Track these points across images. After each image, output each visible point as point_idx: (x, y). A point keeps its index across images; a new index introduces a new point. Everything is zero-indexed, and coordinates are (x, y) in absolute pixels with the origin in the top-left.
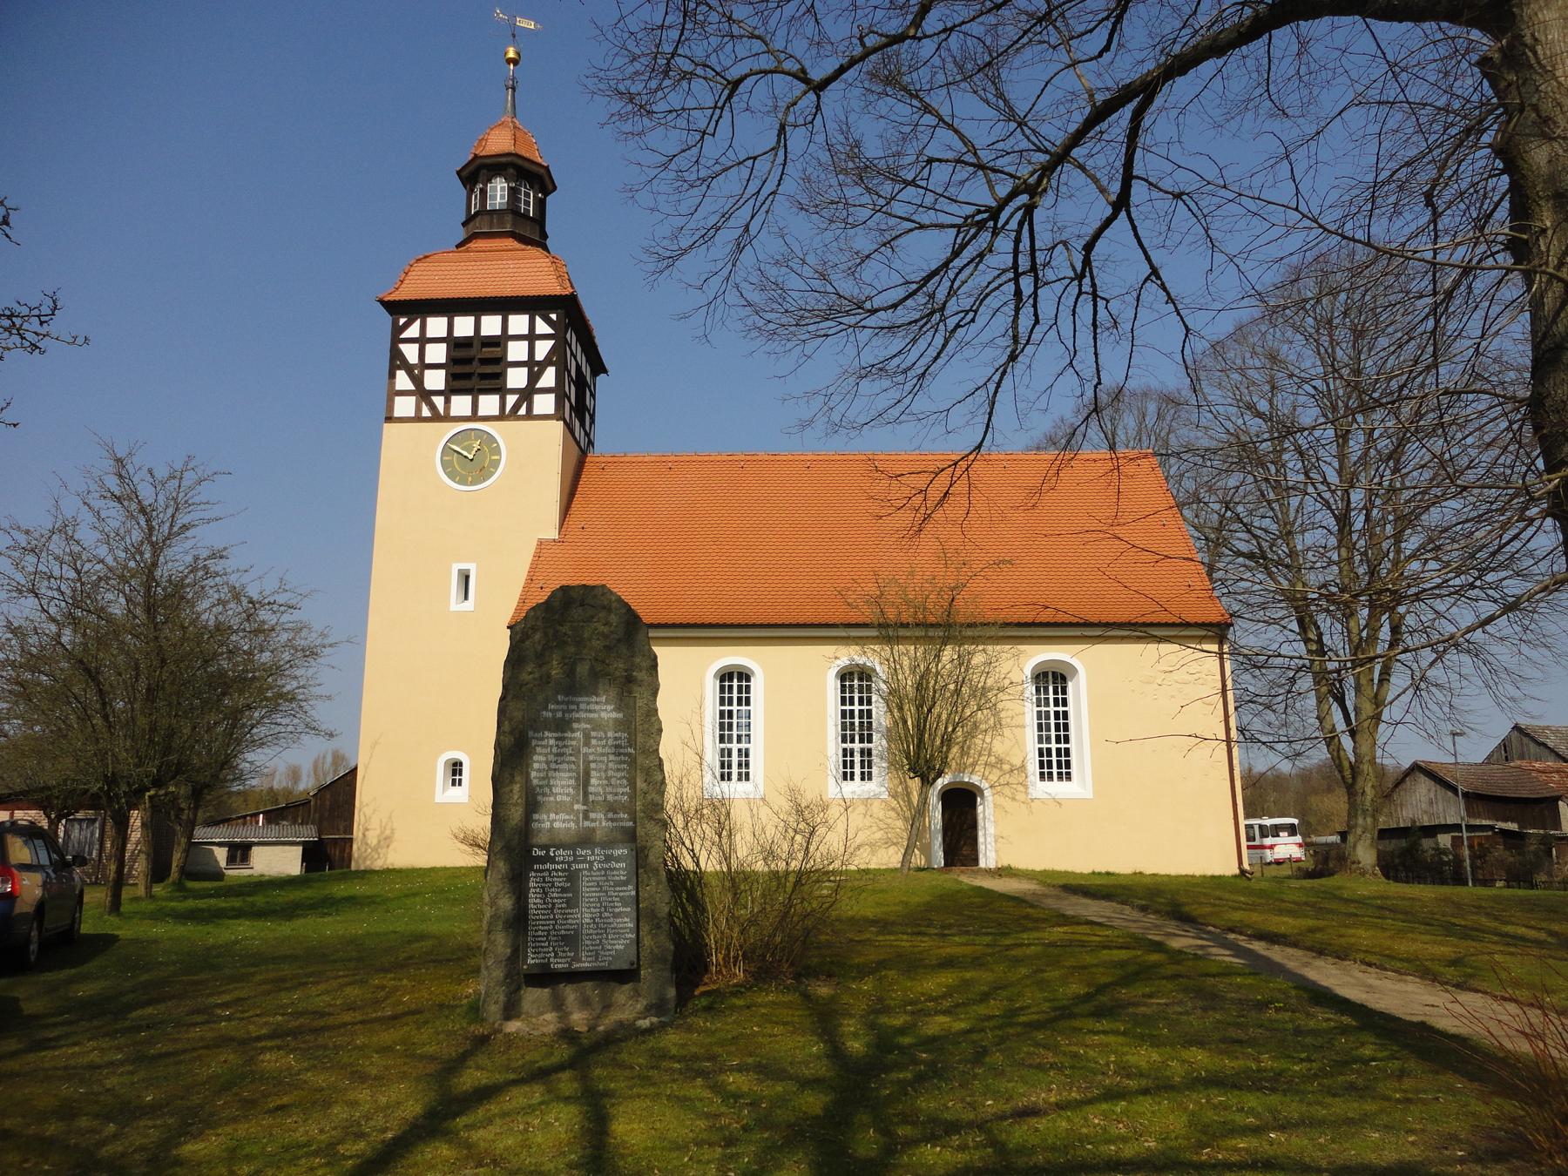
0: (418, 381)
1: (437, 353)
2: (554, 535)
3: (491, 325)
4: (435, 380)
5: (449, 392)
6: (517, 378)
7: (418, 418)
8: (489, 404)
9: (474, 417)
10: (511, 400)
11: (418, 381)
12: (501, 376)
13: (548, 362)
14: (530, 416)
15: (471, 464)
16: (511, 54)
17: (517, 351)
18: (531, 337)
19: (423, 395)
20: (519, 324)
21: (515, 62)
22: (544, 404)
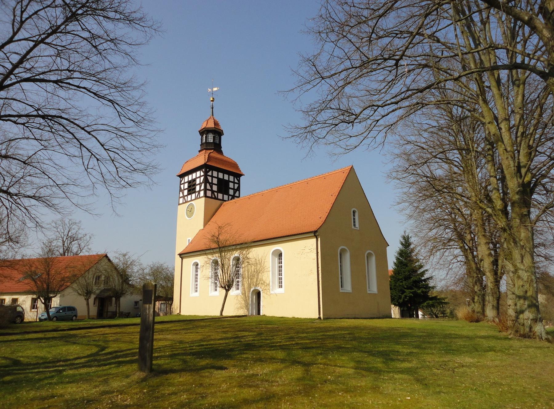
0: (183, 193)
1: (186, 186)
2: (202, 228)
3: (226, 177)
4: (186, 192)
5: (188, 194)
6: (198, 188)
7: (183, 203)
8: (193, 195)
9: (191, 200)
10: (197, 194)
11: (183, 193)
12: (195, 188)
13: (203, 182)
14: (200, 198)
15: (190, 212)
16: (211, 99)
17: (198, 181)
18: (200, 177)
19: (184, 197)
20: (198, 173)
21: (213, 101)
22: (202, 193)
